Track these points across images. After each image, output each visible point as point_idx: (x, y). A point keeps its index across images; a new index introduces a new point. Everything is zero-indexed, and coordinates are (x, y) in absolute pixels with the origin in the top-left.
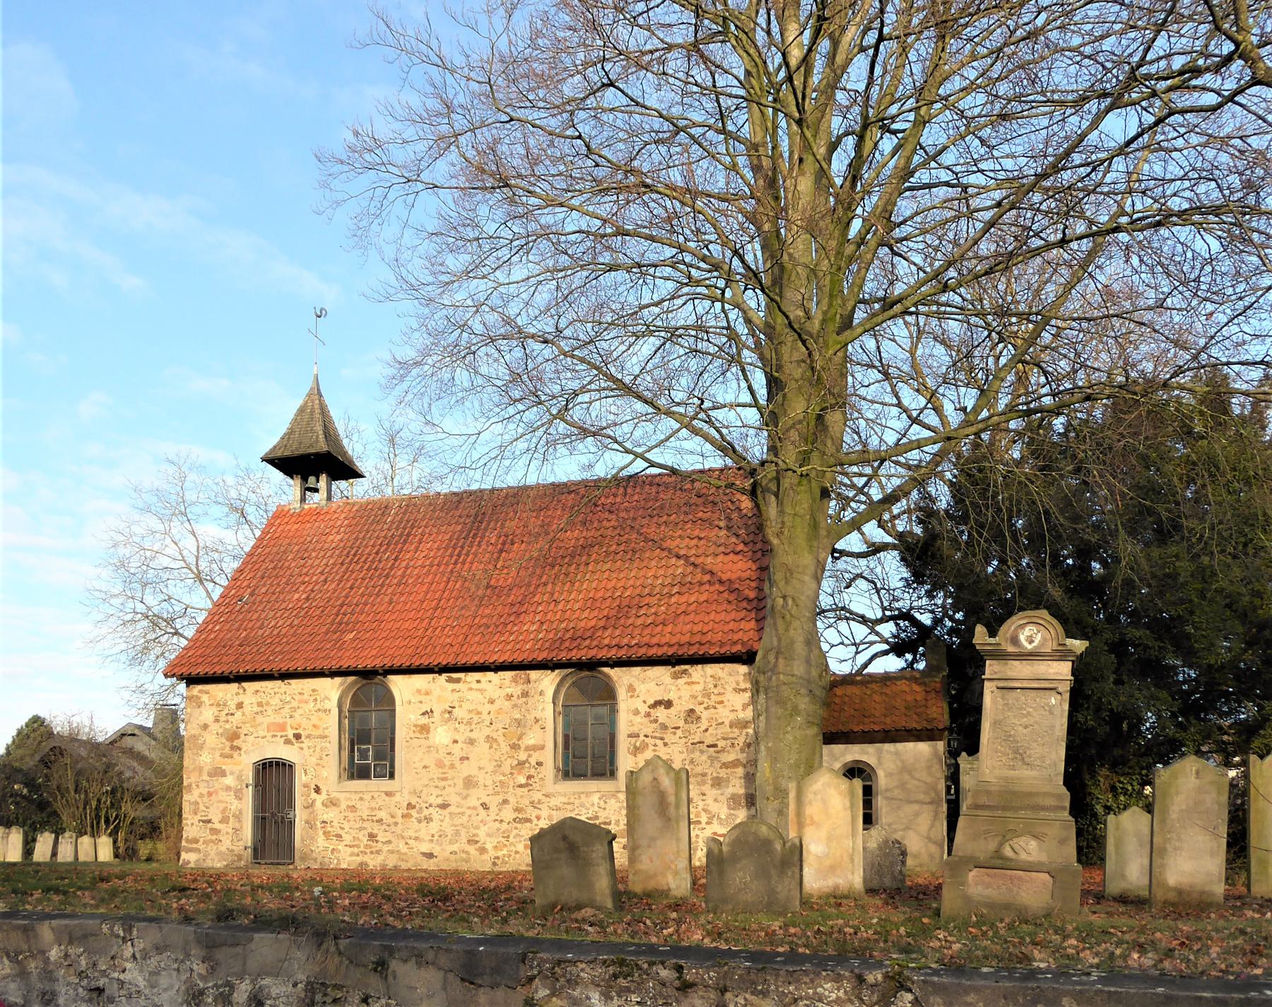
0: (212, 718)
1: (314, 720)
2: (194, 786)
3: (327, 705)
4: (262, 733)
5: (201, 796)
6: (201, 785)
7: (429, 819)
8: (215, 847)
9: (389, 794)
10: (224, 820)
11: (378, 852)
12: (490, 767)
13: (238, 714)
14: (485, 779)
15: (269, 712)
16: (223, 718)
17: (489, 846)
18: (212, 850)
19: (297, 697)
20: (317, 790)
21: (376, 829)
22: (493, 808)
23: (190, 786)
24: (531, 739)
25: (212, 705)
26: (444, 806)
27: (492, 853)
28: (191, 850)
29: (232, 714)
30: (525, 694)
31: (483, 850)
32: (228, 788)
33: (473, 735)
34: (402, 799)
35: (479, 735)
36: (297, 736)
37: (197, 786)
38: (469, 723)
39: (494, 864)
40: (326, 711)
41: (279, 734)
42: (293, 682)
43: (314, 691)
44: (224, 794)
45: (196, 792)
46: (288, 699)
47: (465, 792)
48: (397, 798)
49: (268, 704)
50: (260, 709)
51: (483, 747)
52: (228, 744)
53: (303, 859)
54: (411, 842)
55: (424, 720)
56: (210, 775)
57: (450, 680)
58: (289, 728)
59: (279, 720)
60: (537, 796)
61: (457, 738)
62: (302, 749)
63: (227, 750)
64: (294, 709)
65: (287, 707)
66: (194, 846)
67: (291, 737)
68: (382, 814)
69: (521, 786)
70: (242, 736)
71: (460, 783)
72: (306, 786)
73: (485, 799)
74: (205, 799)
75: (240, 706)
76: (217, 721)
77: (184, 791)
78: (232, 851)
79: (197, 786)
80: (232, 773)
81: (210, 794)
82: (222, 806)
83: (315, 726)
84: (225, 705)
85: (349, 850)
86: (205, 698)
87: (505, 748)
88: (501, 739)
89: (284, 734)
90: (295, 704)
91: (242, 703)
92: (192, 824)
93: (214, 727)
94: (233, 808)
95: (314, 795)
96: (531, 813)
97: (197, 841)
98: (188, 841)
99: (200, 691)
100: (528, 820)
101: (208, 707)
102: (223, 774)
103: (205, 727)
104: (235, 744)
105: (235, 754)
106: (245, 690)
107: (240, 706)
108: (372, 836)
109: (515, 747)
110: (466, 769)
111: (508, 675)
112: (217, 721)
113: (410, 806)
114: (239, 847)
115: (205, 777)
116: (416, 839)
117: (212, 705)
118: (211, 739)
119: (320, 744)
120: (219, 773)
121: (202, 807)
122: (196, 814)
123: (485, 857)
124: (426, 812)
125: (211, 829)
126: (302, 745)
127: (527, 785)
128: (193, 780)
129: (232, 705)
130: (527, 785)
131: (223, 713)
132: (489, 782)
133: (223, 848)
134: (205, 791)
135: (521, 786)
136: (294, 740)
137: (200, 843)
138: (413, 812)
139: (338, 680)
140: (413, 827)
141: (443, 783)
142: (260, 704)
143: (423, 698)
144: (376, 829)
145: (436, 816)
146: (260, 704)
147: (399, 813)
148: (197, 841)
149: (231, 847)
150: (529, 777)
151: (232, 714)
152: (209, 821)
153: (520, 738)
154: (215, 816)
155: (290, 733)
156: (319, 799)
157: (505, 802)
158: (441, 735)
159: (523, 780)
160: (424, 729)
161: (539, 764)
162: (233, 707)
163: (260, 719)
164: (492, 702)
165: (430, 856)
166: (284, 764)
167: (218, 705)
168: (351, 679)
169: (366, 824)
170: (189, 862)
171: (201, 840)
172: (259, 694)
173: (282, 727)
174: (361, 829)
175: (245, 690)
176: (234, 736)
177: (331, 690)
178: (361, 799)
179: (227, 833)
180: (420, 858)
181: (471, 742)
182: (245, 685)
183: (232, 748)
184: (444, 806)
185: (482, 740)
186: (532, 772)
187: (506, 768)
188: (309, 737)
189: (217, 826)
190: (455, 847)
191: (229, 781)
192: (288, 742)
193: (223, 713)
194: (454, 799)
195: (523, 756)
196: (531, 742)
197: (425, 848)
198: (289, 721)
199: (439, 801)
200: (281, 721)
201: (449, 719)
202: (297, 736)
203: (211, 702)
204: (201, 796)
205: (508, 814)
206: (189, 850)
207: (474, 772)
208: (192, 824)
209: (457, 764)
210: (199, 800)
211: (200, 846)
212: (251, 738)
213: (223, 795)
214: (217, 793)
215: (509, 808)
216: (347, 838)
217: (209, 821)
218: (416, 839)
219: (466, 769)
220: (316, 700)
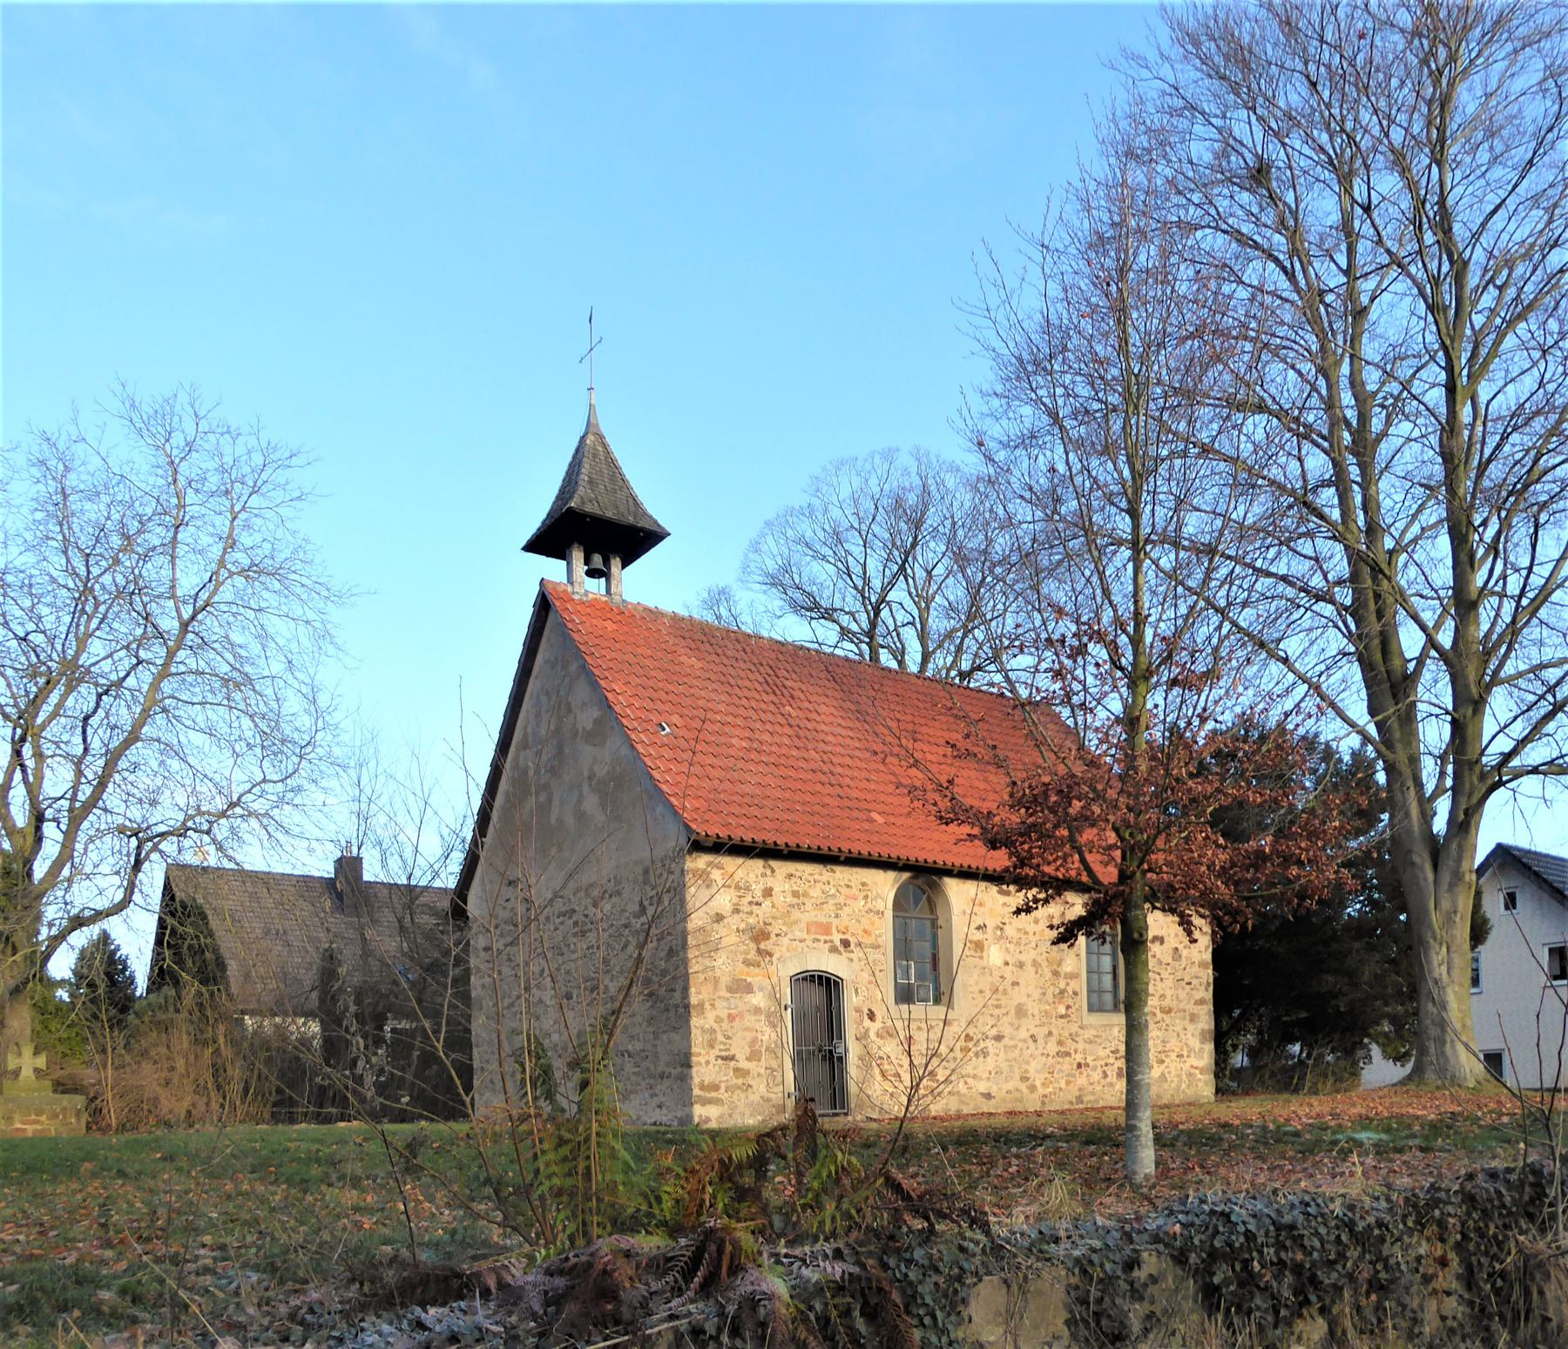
0: (729, 907)
1: (865, 923)
2: (707, 1006)
3: (880, 905)
4: (798, 935)
5: (719, 1020)
6: (718, 1003)
7: (985, 1053)
8: (743, 1096)
10: (754, 1056)
12: (1036, 994)
13: (767, 904)
14: (1033, 1008)
15: (809, 906)
17: (1038, 1083)
18: (739, 1098)
19: (844, 890)
20: (872, 1016)
22: (1041, 1041)
23: (701, 1005)
26: (999, 1038)
27: (1041, 1091)
28: (709, 1101)
29: (758, 904)
31: (1033, 1088)
32: (757, 1010)
33: (1023, 958)
35: (1027, 957)
37: (713, 1005)
38: (1018, 944)
39: (1043, 1103)
40: (880, 913)
41: (823, 938)
42: (839, 869)
43: (864, 884)
44: (753, 1018)
45: (711, 1015)
47: (1016, 1022)
49: (805, 894)
50: (795, 900)
51: (1029, 969)
52: (753, 945)
53: (861, 1106)
54: (970, 1080)
55: (977, 936)
56: (730, 990)
57: (1001, 892)
58: (834, 930)
60: (1074, 1028)
63: (753, 955)
64: (839, 907)
65: (831, 902)
66: (713, 1094)
67: (838, 943)
70: (773, 936)
71: (1013, 1012)
72: (858, 1010)
73: (1034, 1031)
74: (725, 1025)
75: (768, 892)
76: (736, 911)
77: (693, 1013)
78: (768, 1100)
79: (713, 1005)
80: (761, 989)
81: (731, 1018)
82: (749, 1036)
83: (865, 932)
84: (748, 889)
86: (716, 875)
87: (1048, 975)
88: (1045, 964)
90: (841, 900)
91: (771, 889)
92: (708, 1063)
94: (765, 1038)
95: (867, 1022)
96: (1071, 1046)
97: (716, 1088)
98: (702, 1087)
99: (709, 864)
100: (1068, 1054)
102: (749, 989)
103: (719, 918)
104: (762, 946)
106: (773, 871)
107: (768, 892)
109: (1056, 974)
110: (1018, 996)
112: (736, 911)
114: (777, 1095)
115: (723, 993)
116: (975, 1077)
118: (728, 934)
119: (874, 955)
120: (741, 987)
121: (720, 1038)
122: (712, 1047)
123: (1035, 1096)
124: (982, 1045)
125: (736, 1070)
127: (1066, 1016)
128: (704, 995)
129: (757, 890)
130: (1066, 1016)
131: (745, 901)
132: (1036, 1012)
133: (754, 1098)
134: (724, 1013)
136: (841, 949)
137: (723, 1090)
138: (970, 1045)
139: (891, 875)
141: (997, 1012)
142: (795, 894)
145: (991, 1050)
146: (795, 894)
148: (716, 1088)
149: (766, 1095)
150: (1068, 1007)
151: (758, 904)
152: (732, 1058)
153: (1059, 964)
154: (740, 1050)
155: (837, 938)
156: (874, 1027)
157: (1050, 1033)
158: (995, 955)
159: (1062, 1010)
160: (979, 946)
161: (1075, 993)
162: (759, 893)
163: (796, 914)
165: (988, 1096)
166: (828, 979)
167: (738, 887)
168: (906, 875)
170: (708, 1120)
171: (723, 1086)
173: (826, 929)
175: (773, 871)
176: (760, 935)
177: (885, 884)
180: (981, 1100)
181: (1021, 965)
182: (774, 863)
183: (759, 951)
184: (999, 1038)
185: (1029, 964)
186: (1070, 1002)
187: (1049, 997)
189: (743, 1064)
190: (1010, 1086)
191: (758, 999)
192: (834, 950)
193: (745, 901)
194: (1007, 1030)
195: (1062, 986)
196: (1069, 969)
197: (982, 1087)
198: (835, 922)
199: (994, 1032)
200: (824, 920)
201: (1001, 937)
202: (846, 944)
204: (719, 1020)
205: (1052, 1048)
206: (706, 1102)
207: (1023, 1000)
208: (708, 1063)
209: (1009, 989)
210: (715, 1026)
211: (722, 1094)
212: (785, 941)
213: (750, 1020)
214: (741, 1015)
215: (1053, 1040)
217: (732, 1058)
218: (975, 1077)
219: (1018, 996)
220: (866, 897)
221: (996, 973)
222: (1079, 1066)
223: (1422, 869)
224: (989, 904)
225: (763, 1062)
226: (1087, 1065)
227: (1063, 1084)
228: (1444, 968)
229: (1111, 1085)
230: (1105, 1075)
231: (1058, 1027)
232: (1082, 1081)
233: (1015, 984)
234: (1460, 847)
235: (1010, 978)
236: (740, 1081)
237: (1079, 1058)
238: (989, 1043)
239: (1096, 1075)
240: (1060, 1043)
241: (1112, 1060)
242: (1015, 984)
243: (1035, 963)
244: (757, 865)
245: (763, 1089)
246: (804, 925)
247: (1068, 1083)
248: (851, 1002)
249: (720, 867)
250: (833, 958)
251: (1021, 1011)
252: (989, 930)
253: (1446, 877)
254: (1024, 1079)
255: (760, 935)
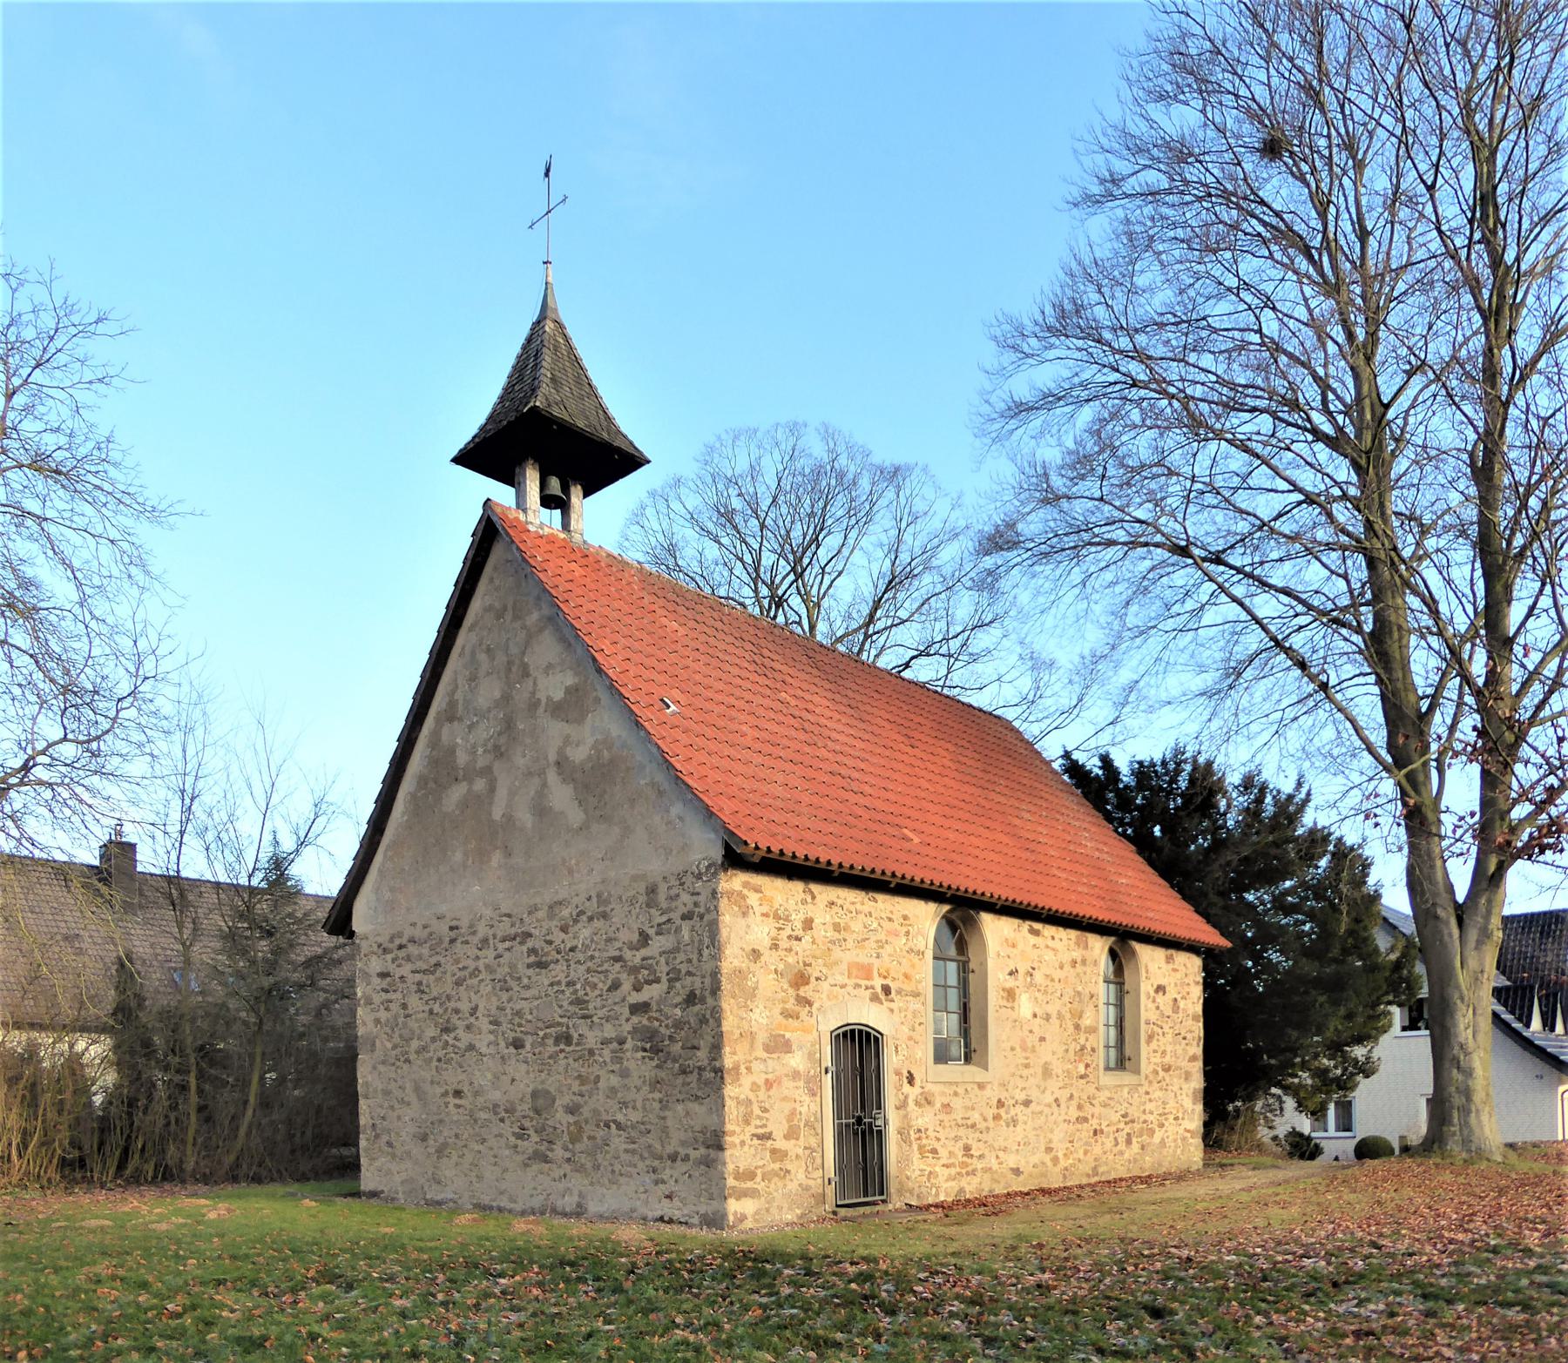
0: (767, 942)
2: (743, 1070)
4: (841, 979)
5: (755, 1087)
6: (756, 1066)
8: (780, 1184)
9: (981, 1086)
10: (791, 1134)
11: (973, 1172)
12: (1060, 1053)
14: (1058, 1067)
15: (850, 944)
16: (784, 944)
17: (1060, 1155)
19: (886, 924)
20: (911, 1080)
21: (971, 1138)
22: (1063, 1105)
23: (736, 1068)
24: (1087, 1021)
25: (765, 915)
27: (1063, 1163)
29: (798, 939)
30: (1084, 962)
31: (1055, 1160)
32: (796, 1075)
34: (992, 1094)
36: (887, 990)
38: (1046, 992)
39: (1065, 1177)
41: (864, 983)
42: (880, 897)
43: (905, 918)
44: (791, 1084)
45: (746, 1081)
46: (875, 925)
47: (1043, 1084)
48: (988, 1092)
50: (837, 935)
51: (1054, 1021)
52: (791, 992)
53: (900, 1192)
54: (1001, 1154)
56: (767, 1049)
58: (875, 974)
59: (863, 959)
61: (1037, 1010)
62: (892, 1010)
63: (791, 1005)
64: (881, 944)
66: (749, 1184)
67: (879, 990)
68: (975, 1117)
69: (1082, 1077)
70: (813, 980)
71: (1039, 1071)
73: (1057, 1094)
74: (762, 1094)
75: (808, 924)
76: (775, 947)
77: (728, 1079)
78: (807, 1188)
79: (748, 1069)
81: (769, 1084)
82: (787, 1107)
83: (906, 976)
84: (787, 919)
85: (946, 1172)
86: (753, 899)
87: (1071, 1029)
88: (1068, 1016)
89: (869, 983)
90: (882, 937)
92: (743, 1143)
93: (770, 958)
94: (804, 1110)
95: (907, 1088)
97: (751, 1175)
99: (746, 885)
100: (1086, 1120)
101: (759, 918)
103: (756, 954)
105: (804, 1012)
106: (814, 898)
107: (808, 924)
108: (967, 1148)
109: (1077, 1027)
110: (1045, 1054)
111: (1073, 934)
113: (1000, 1104)
114: (816, 1184)
115: (760, 1053)
117: (765, 915)
118: (766, 981)
119: (915, 1005)
120: (778, 1045)
121: (757, 1111)
122: (747, 1122)
125: (774, 1151)
126: (892, 1005)
128: (740, 1057)
129: (797, 919)
133: (793, 1186)
134: (761, 1081)
135: (1082, 1077)
136: (882, 997)
137: (759, 1179)
138: (1002, 1111)
140: (1002, 1135)
141: (1025, 1072)
142: (837, 928)
143: (1010, 951)
144: (971, 1138)
145: (1021, 1118)
147: (990, 1113)
149: (805, 1182)
150: (1087, 1066)
151: (798, 939)
154: (778, 1127)
155: (878, 983)
156: (913, 1092)
157: (1072, 1096)
158: (1025, 1006)
161: (1093, 1050)
162: (799, 925)
163: (837, 953)
164: (1061, 967)
165: (1017, 1172)
166: (868, 1034)
167: (777, 917)
168: (946, 908)
169: (962, 1132)
170: (743, 1218)
171: (759, 1172)
172: (835, 909)
173: (866, 971)
174: (957, 1139)
175: (814, 898)
176: (801, 980)
178: (956, 1094)
179: (797, 1156)
182: (815, 887)
184: (1027, 1103)
185: (1054, 1016)
188: (899, 992)
189: (780, 1144)
190: (1035, 1159)
191: (797, 1061)
192: (875, 998)
194: (1034, 1094)
195: (1082, 1041)
197: (1012, 1161)
199: (1021, 1097)
201: (1031, 984)
202: (887, 990)
203: (765, 909)
207: (1049, 1058)
208: (743, 1143)
210: (752, 1096)
212: (825, 986)
213: (788, 1084)
214: (778, 1081)
215: (1074, 1103)
216: (943, 1153)
219: (1045, 1054)
220: (908, 933)
221: (1026, 1028)
222: (1095, 1132)
223: (1447, 923)
224: (1020, 946)
225: (801, 1142)
226: (1102, 1132)
227: (1081, 1155)
228: (1470, 1031)
229: (1121, 1153)
230: (1117, 1144)
231: (1082, 1090)
232: (1097, 1150)
233: (1042, 1039)
234: (1489, 901)
235: (1038, 1032)
236: (777, 1166)
237: (1094, 1123)
238: (1020, 1108)
239: (1109, 1143)
240: (1080, 1107)
241: (1122, 1126)
242: (1042, 1039)
243: (1060, 1016)
244: (797, 887)
245: (801, 1176)
246: (844, 967)
247: (1086, 1153)
248: (892, 1061)
249: (757, 890)
250: (875, 1007)
251: (1047, 1072)
252: (1021, 976)
253: (1473, 935)
254: (1049, 1150)
255: (801, 980)
